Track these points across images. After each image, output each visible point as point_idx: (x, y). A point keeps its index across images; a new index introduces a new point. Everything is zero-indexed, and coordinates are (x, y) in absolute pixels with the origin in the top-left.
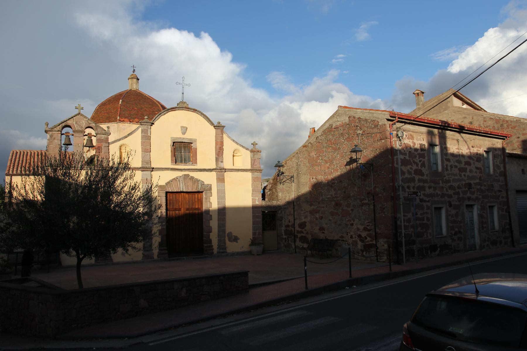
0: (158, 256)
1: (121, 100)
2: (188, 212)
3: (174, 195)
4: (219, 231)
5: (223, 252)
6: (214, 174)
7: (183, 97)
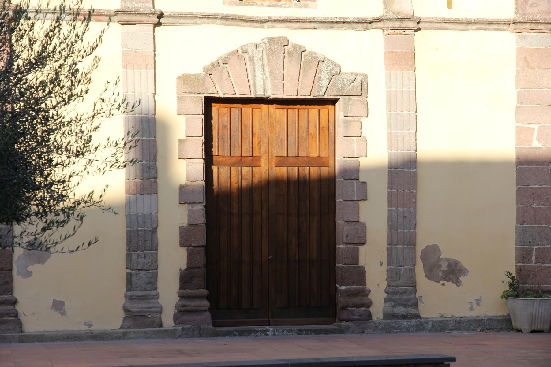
0: (176, 319)
3: (236, 109)
5: (404, 317)
6: (376, 35)
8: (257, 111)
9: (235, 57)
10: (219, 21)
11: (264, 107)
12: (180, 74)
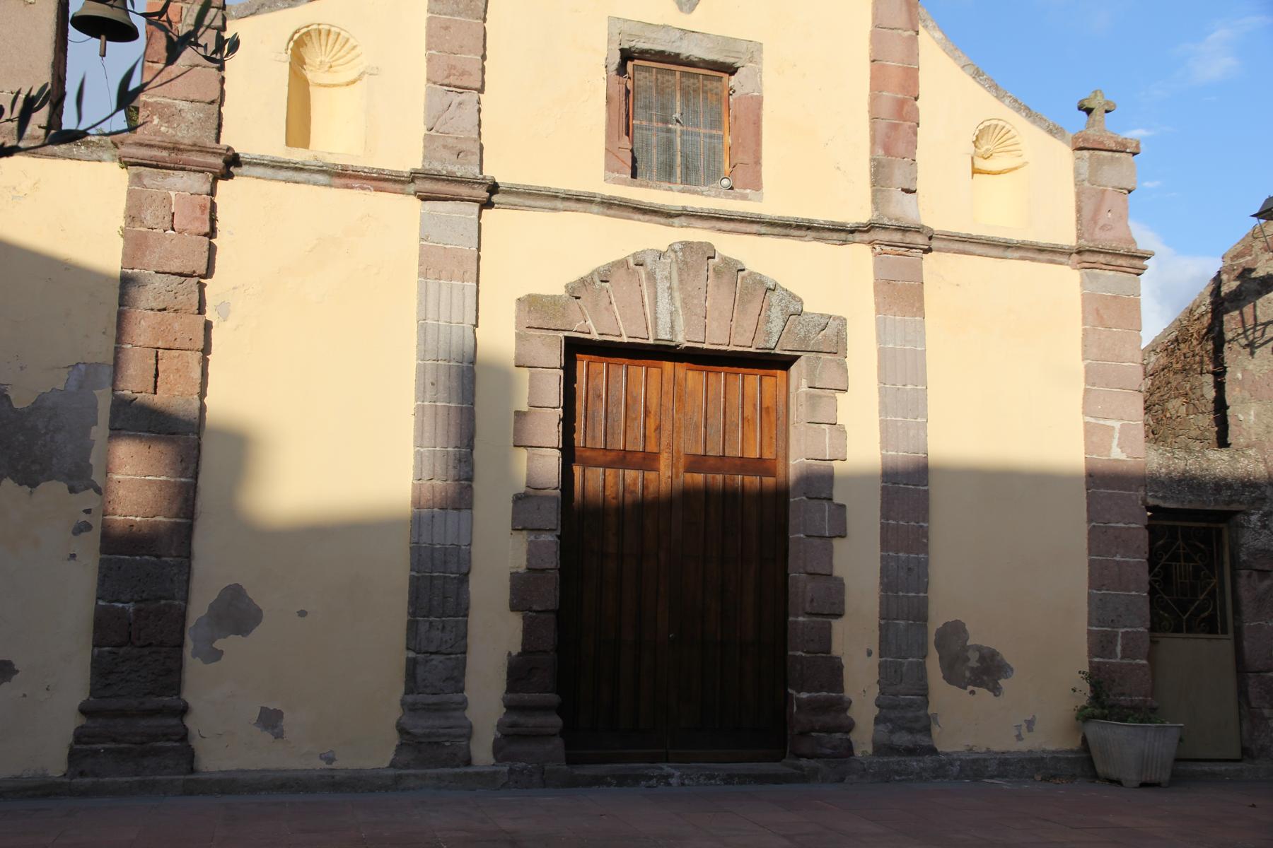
0: (498, 750)
2: (699, 478)
4: (886, 615)
5: (911, 751)
6: (860, 255)
8: (654, 372)
9: (623, 271)
10: (595, 208)
11: (668, 365)
12: (522, 294)
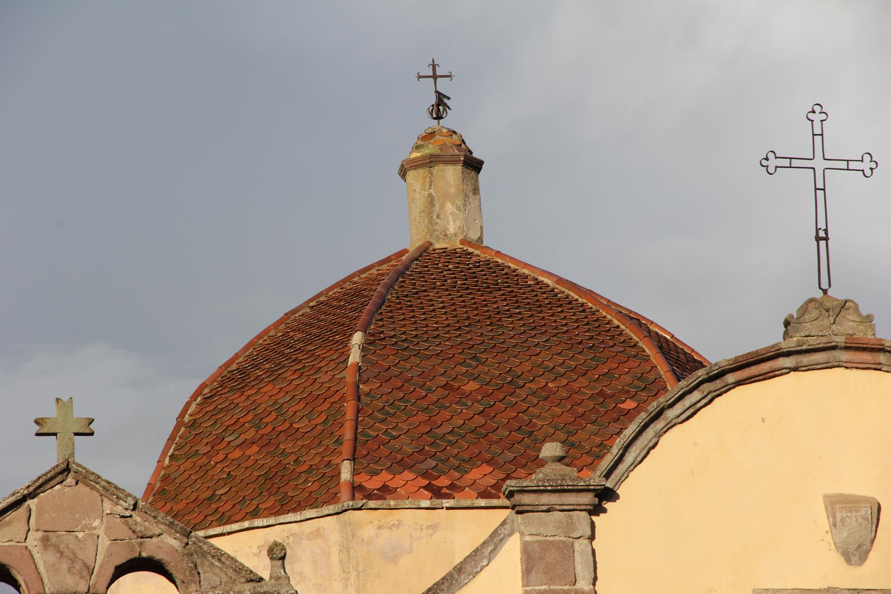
1: (357, 338)
7: (823, 267)
